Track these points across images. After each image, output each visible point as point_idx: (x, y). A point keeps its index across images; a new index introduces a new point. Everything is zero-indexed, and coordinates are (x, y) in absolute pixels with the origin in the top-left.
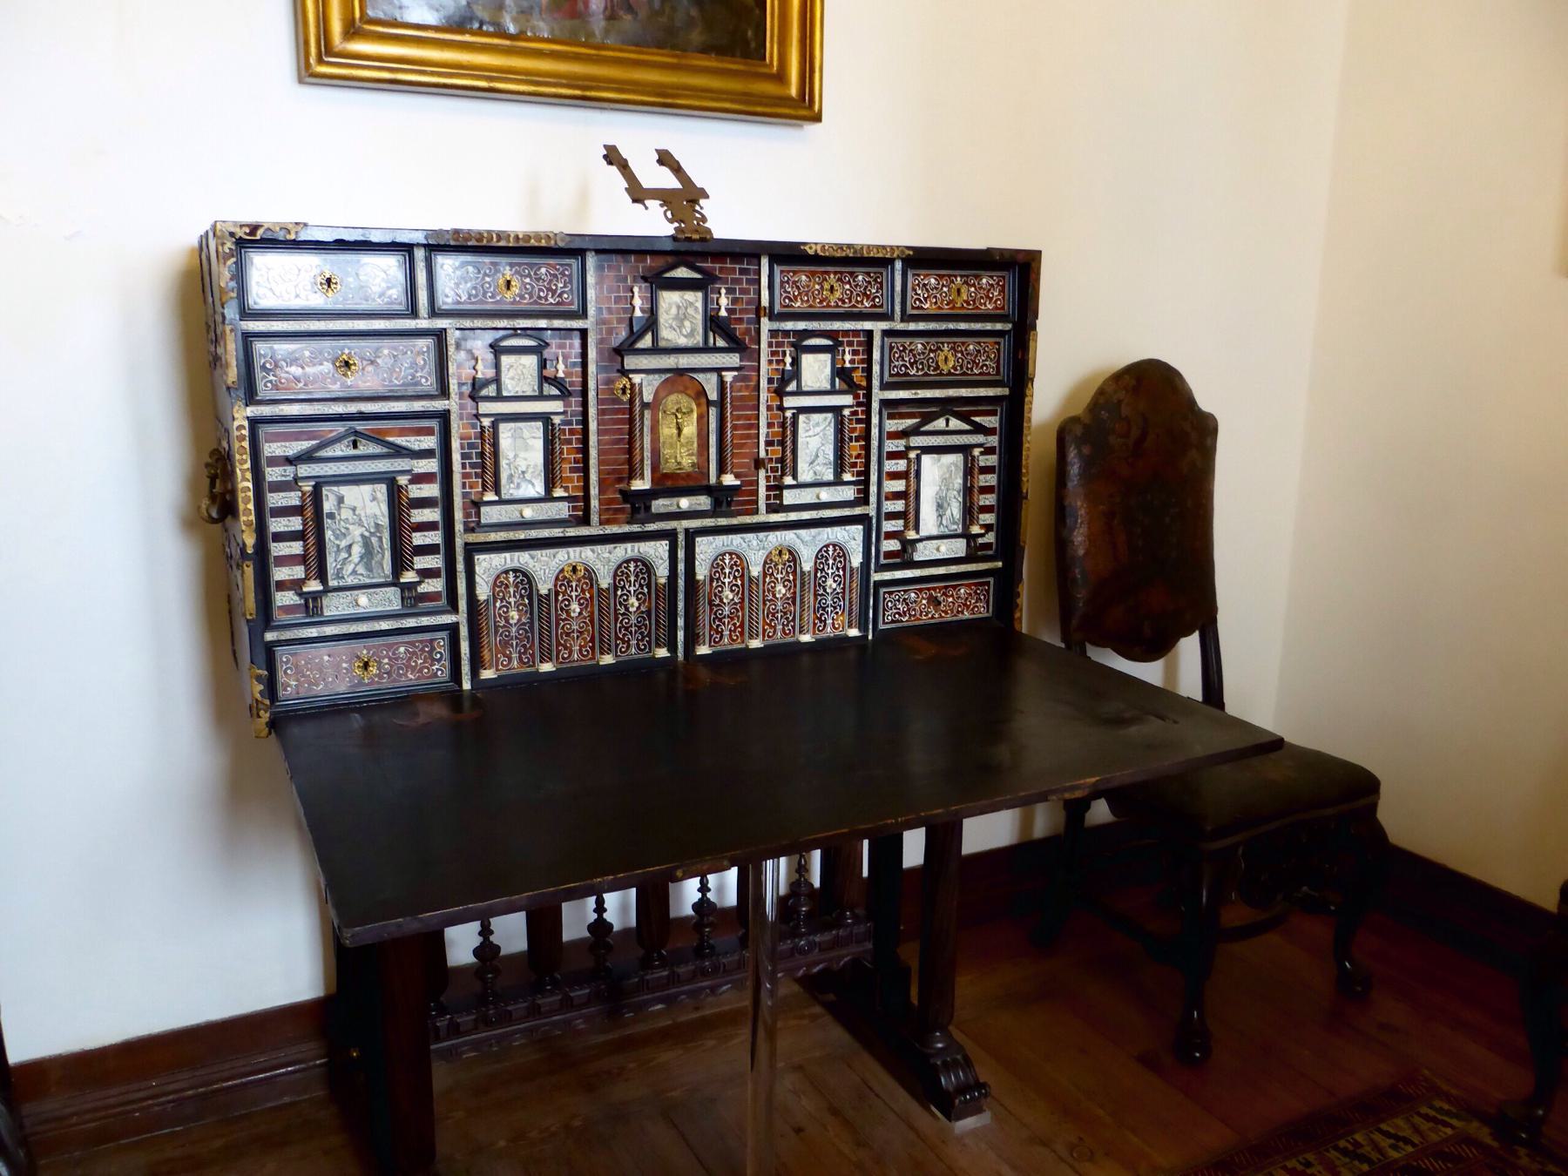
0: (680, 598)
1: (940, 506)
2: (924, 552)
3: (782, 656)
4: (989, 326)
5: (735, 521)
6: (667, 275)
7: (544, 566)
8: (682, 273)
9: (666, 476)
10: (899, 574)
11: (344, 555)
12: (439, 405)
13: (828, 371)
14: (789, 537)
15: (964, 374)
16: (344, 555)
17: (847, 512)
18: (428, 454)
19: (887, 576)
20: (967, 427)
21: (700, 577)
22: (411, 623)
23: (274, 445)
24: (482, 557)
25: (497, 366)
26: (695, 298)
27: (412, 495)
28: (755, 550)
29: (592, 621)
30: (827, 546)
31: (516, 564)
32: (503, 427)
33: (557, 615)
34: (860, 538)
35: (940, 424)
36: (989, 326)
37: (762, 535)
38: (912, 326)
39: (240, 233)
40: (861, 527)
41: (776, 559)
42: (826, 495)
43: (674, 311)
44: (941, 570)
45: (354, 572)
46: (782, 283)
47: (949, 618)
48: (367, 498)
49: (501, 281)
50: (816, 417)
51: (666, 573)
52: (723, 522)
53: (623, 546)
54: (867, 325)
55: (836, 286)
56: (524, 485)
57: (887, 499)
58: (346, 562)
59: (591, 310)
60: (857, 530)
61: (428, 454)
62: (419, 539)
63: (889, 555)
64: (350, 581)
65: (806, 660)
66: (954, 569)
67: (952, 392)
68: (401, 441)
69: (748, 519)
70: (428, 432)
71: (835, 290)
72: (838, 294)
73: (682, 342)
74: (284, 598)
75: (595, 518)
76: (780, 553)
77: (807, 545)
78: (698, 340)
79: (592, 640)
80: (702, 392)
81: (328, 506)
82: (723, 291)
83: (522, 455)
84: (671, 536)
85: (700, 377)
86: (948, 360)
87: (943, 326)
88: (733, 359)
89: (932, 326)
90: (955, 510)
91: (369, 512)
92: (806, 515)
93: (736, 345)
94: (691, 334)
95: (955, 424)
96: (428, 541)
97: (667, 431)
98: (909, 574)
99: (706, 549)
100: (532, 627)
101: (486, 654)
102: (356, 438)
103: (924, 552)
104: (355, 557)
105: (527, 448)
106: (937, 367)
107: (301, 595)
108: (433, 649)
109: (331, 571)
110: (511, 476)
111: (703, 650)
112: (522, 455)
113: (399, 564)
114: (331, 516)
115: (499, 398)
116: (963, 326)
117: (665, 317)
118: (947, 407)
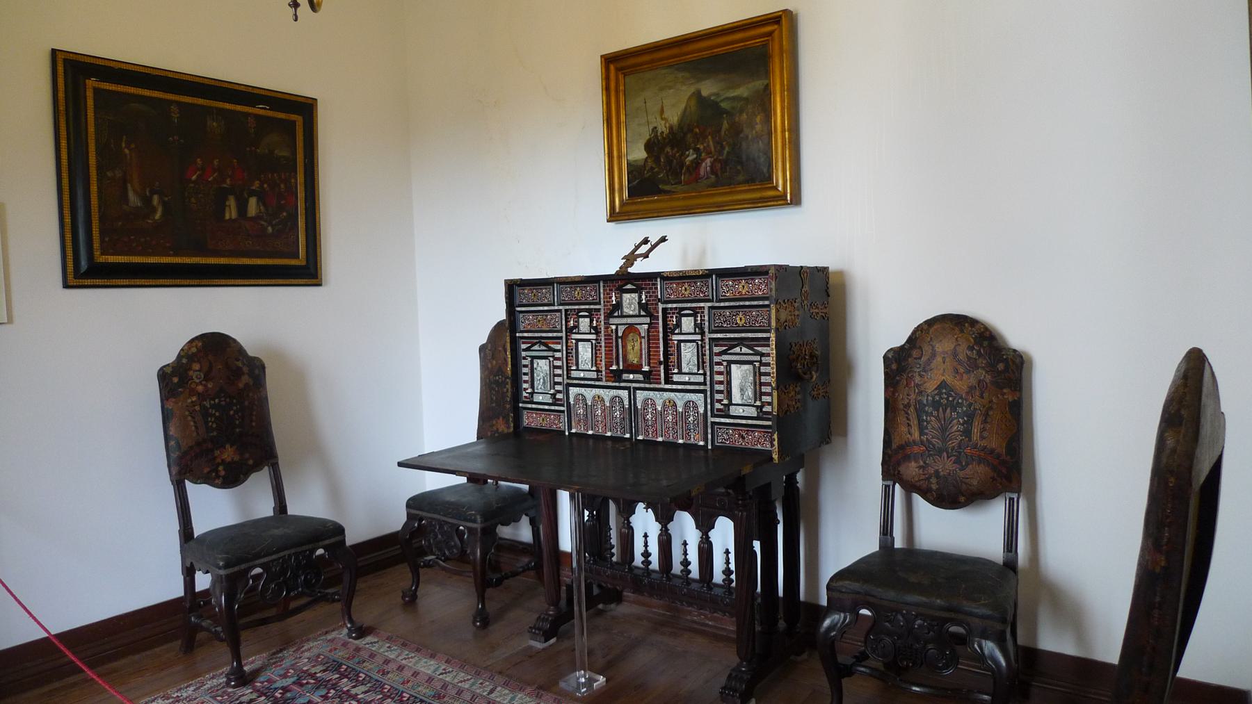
0: (632, 412)
2: (734, 411)
3: (670, 446)
4: (761, 303)
7: (589, 393)
8: (629, 286)
10: (723, 420)
14: (672, 394)
17: (697, 387)
19: (717, 420)
26: (635, 296)
28: (659, 399)
35: (737, 350)
38: (722, 304)
42: (694, 379)
44: (744, 422)
54: (702, 305)
58: (539, 386)
63: (718, 410)
65: (681, 451)
66: (750, 422)
67: (743, 335)
71: (686, 290)
77: (680, 400)
78: (637, 312)
86: (740, 320)
87: (737, 304)
88: (648, 320)
90: (750, 392)
92: (680, 387)
93: (650, 315)
95: (745, 350)
97: (629, 348)
98: (728, 421)
99: (641, 395)
103: (734, 411)
111: (640, 438)
116: (747, 303)
117: (625, 304)
118: (741, 342)
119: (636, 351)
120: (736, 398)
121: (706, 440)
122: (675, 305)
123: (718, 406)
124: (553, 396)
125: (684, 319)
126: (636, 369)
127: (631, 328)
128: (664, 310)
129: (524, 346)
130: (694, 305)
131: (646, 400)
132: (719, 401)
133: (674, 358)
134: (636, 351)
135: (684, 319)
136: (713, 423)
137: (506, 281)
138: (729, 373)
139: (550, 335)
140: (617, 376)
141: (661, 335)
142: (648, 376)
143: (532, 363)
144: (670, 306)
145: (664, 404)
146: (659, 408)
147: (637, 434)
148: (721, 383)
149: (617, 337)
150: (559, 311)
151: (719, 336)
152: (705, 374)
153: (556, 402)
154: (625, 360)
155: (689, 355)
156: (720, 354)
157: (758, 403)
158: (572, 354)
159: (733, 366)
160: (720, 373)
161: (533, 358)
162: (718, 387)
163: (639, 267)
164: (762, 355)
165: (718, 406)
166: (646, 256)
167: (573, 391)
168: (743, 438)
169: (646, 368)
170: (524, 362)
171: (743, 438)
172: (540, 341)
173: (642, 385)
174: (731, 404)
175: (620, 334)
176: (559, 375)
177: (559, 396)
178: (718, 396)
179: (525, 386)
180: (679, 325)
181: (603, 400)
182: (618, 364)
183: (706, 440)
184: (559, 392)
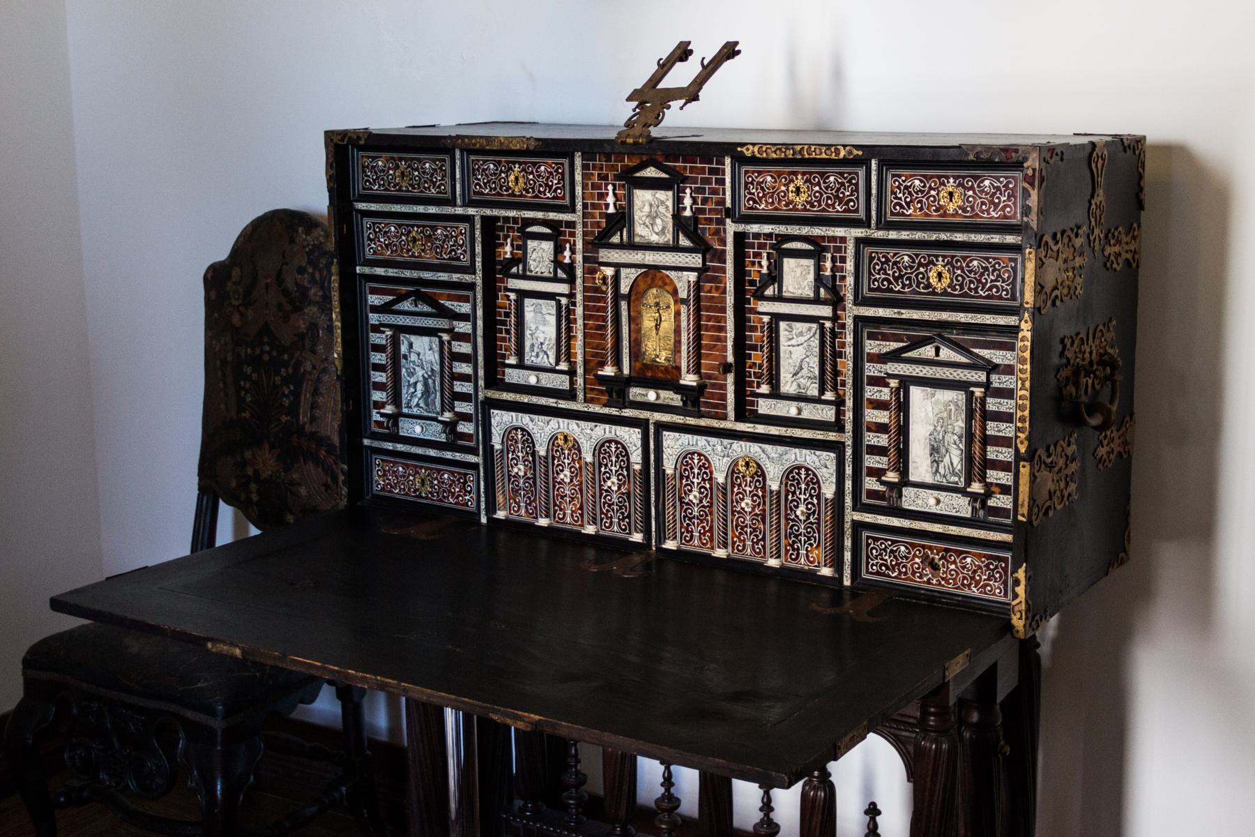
1: (934, 450)
4: (996, 239)
5: (703, 422)
6: (638, 175)
7: (542, 429)
8: (651, 172)
9: (646, 366)
10: (883, 520)
11: (412, 390)
12: (468, 278)
13: (811, 277)
14: (754, 449)
15: (965, 295)
16: (412, 390)
17: (819, 435)
18: (463, 317)
19: (868, 518)
20: (964, 360)
21: (669, 471)
22: (448, 455)
23: (374, 297)
24: (496, 412)
25: (524, 248)
26: (666, 196)
27: (454, 350)
28: (721, 456)
29: (581, 490)
30: (799, 468)
31: (519, 424)
32: (527, 301)
33: (554, 478)
34: (833, 467)
35: (928, 352)
36: (996, 239)
37: (726, 442)
38: (893, 235)
39: (336, 139)
40: (833, 455)
41: (743, 469)
43: (647, 209)
45: (418, 405)
46: (746, 184)
47: (949, 588)
48: (427, 347)
49: (512, 177)
50: (800, 326)
51: (639, 460)
52: (691, 421)
53: (603, 426)
54: (840, 232)
55: (804, 188)
56: (541, 354)
57: (869, 430)
58: (413, 397)
59: (579, 206)
60: (829, 457)
61: (463, 317)
62: (460, 387)
63: (872, 494)
64: (415, 411)
65: (772, 588)
66: (954, 530)
67: (945, 316)
68: (448, 304)
69: (715, 423)
70: (466, 299)
71: (798, 193)
72: (804, 197)
73: (654, 239)
74: (376, 417)
75: (581, 396)
76: (747, 464)
77: (775, 463)
78: (668, 238)
79: (581, 508)
80: (675, 292)
81: (404, 349)
82: (688, 191)
83: (541, 328)
84: (641, 424)
85: (672, 274)
88: (696, 260)
89: (918, 235)
90: (955, 457)
91: (428, 359)
92: (774, 430)
93: (700, 246)
94: (663, 231)
95: (946, 354)
96: (465, 390)
97: (648, 323)
98: (895, 522)
99: (674, 444)
100: (535, 482)
101: (500, 499)
102: (420, 297)
103: (912, 499)
104: (419, 394)
105: (545, 323)
106: (928, 286)
107: (383, 415)
108: (465, 482)
109: (404, 401)
110: (533, 345)
111: (670, 545)
112: (541, 328)
113: (447, 405)
114: (405, 357)
115: (524, 277)
116: (959, 237)
119: (661, 331)
120: (920, 468)
121: (838, 564)
122: (767, 229)
123: (870, 483)
124: (450, 427)
125: (789, 264)
126: (665, 378)
127: (653, 275)
128: (740, 238)
129: (374, 300)
130: (817, 231)
131: (686, 458)
132: (877, 473)
133: (758, 358)
134: (661, 331)
135: (789, 264)
136: (858, 526)
137: (326, 132)
138: (903, 407)
139: (444, 276)
140: (616, 390)
141: (730, 300)
142: (693, 399)
143: (396, 343)
144: (755, 228)
145: (733, 471)
146: (720, 478)
147: (661, 539)
148: (881, 428)
149: (617, 296)
150: (468, 219)
151: (882, 312)
152: (839, 403)
153: (455, 440)
154: (636, 353)
155: (798, 353)
156: (882, 358)
157: (976, 487)
158: (500, 329)
159: (916, 393)
160: (879, 405)
161: (399, 330)
162: (871, 439)
163: (678, 121)
164: (992, 368)
165: (870, 483)
166: (691, 94)
167: (501, 420)
168: (935, 567)
169: (689, 380)
170: (376, 338)
171: (935, 567)
172: (420, 291)
173: (678, 419)
174: (905, 482)
175: (624, 289)
176: (464, 378)
177: (466, 428)
178: (870, 461)
179: (377, 396)
180: (775, 276)
181: (577, 447)
182: (618, 363)
183: (838, 564)
184: (465, 417)
